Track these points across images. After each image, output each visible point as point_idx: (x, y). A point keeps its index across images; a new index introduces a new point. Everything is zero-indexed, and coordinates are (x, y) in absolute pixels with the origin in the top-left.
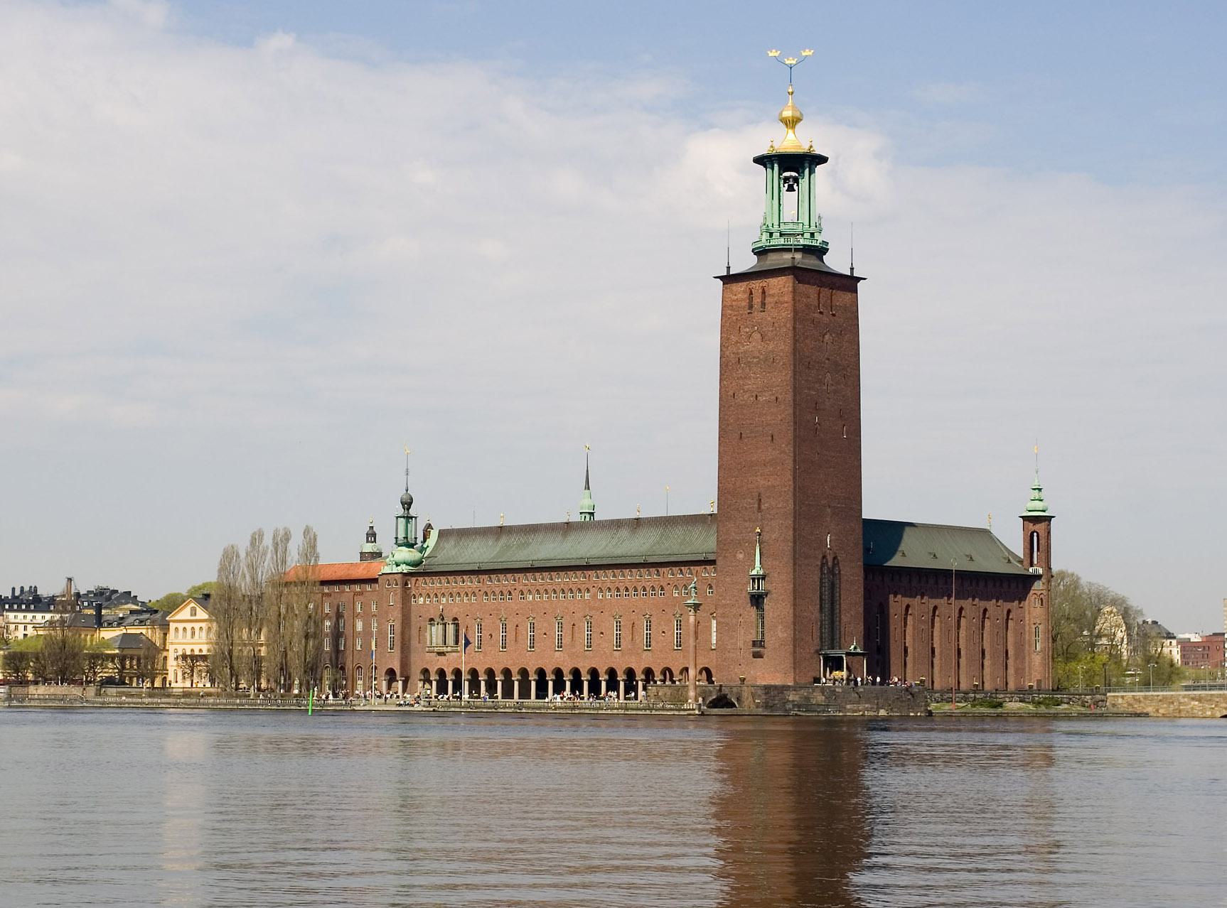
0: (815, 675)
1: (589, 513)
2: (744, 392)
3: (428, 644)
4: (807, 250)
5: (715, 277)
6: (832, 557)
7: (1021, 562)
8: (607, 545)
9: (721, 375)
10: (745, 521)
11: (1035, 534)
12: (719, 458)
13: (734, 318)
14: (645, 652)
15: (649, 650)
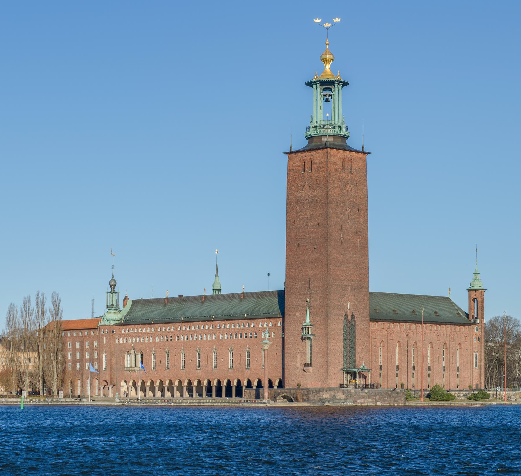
0: (340, 383)
1: (218, 290)
2: (300, 220)
3: (126, 366)
4: (335, 136)
5: (283, 153)
6: (351, 315)
7: (467, 315)
8: (226, 309)
9: (287, 210)
10: (300, 294)
11: (476, 300)
12: (286, 258)
13: (294, 177)
14: (247, 370)
15: (248, 369)
